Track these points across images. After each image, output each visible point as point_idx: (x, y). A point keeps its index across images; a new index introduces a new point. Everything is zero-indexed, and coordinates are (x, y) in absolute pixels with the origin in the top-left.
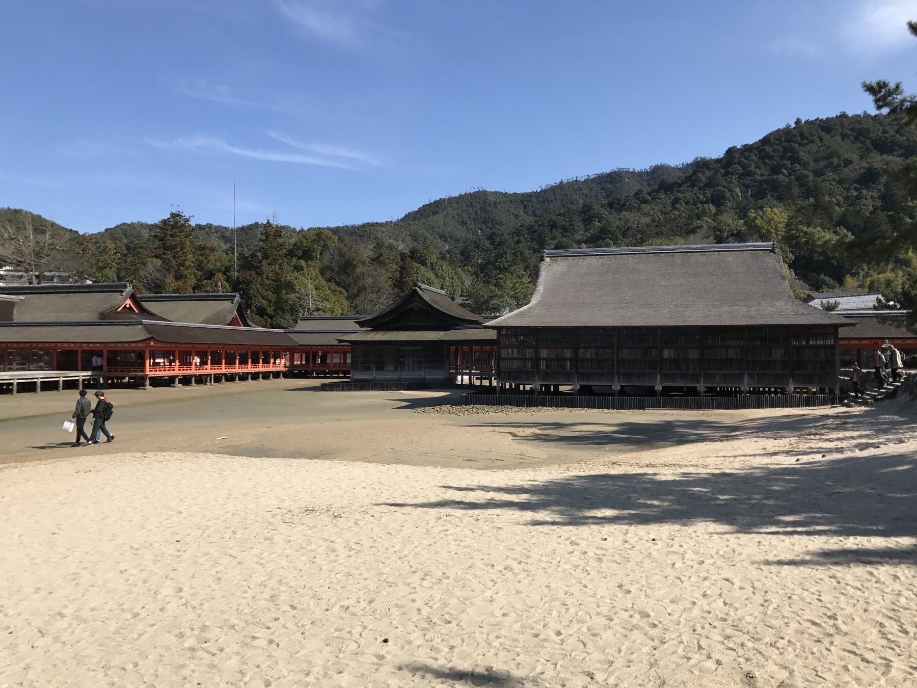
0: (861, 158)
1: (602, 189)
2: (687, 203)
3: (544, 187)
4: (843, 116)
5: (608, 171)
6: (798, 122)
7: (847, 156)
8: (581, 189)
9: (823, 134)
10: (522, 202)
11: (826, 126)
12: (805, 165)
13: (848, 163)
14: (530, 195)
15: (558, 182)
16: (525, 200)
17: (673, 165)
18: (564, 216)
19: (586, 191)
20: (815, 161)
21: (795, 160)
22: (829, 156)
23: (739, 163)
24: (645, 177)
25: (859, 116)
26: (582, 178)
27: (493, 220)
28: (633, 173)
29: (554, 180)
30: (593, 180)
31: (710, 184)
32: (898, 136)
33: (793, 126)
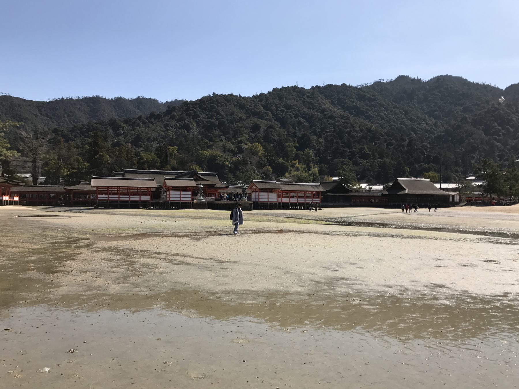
0: (248, 118)
1: (88, 106)
2: (172, 127)
3: (51, 100)
4: (232, 95)
6: (214, 94)
7: (239, 115)
8: (75, 104)
9: (226, 102)
10: (38, 107)
11: (229, 99)
12: (223, 116)
13: (241, 119)
14: (43, 103)
15: (61, 98)
16: (40, 105)
17: (127, 98)
18: (101, 124)
19: (79, 106)
20: (226, 115)
21: (218, 113)
22: (232, 114)
23: (192, 110)
26: (75, 97)
27: (20, 115)
28: (105, 99)
29: (58, 97)
31: (181, 119)
32: (256, 109)
33: (212, 95)
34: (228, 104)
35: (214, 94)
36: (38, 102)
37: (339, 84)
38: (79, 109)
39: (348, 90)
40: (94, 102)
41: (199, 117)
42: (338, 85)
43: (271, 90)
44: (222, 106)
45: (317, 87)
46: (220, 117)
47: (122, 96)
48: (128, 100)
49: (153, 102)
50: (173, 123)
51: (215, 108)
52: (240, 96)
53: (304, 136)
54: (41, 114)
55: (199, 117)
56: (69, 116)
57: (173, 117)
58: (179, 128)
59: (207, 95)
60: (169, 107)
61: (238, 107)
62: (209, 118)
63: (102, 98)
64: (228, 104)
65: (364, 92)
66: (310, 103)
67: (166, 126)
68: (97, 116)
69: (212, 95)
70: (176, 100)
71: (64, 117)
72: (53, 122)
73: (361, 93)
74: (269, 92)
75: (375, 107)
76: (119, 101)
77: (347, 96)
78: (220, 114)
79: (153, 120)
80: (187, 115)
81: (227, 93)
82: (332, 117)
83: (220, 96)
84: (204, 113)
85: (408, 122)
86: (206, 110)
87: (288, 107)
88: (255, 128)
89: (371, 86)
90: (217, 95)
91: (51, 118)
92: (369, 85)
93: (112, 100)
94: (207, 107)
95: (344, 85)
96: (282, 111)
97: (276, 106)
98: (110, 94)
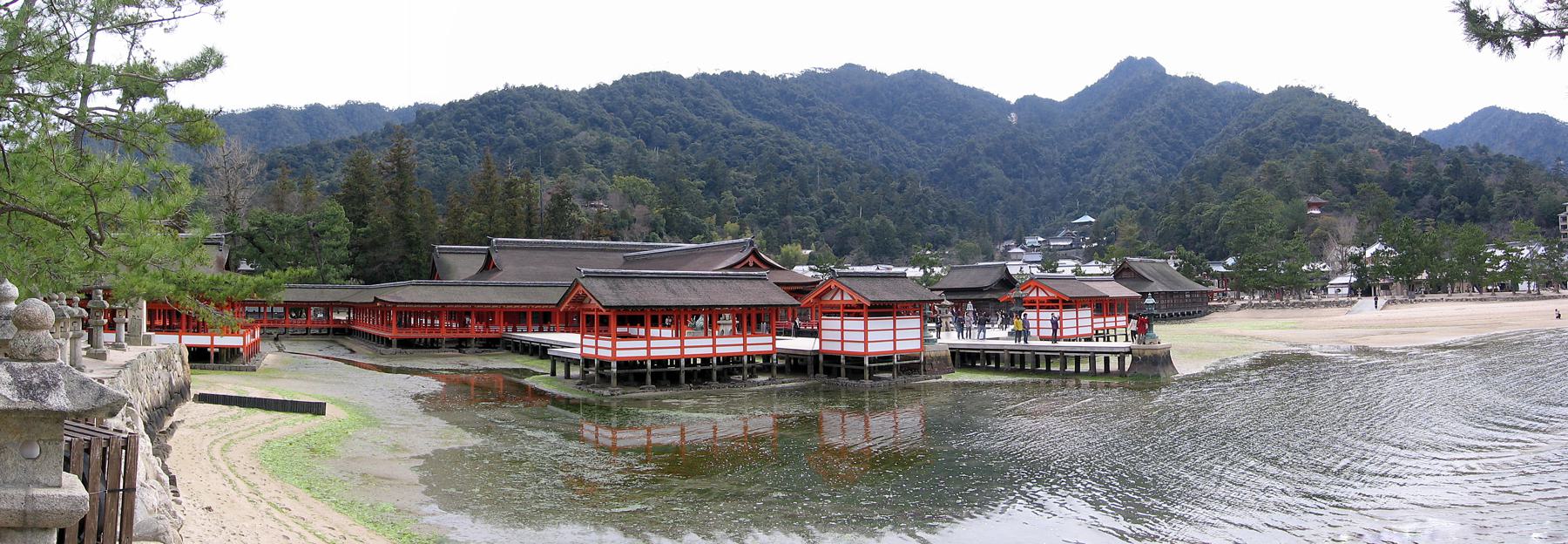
13: (568, 134)
37: (746, 72)
43: (618, 78)
45: (704, 75)
53: (712, 166)
60: (418, 113)
66: (696, 105)
73: (783, 89)
74: (616, 83)
75: (814, 115)
82: (748, 132)
85: (878, 149)
87: (657, 110)
88: (604, 149)
96: (647, 118)
97: (631, 107)
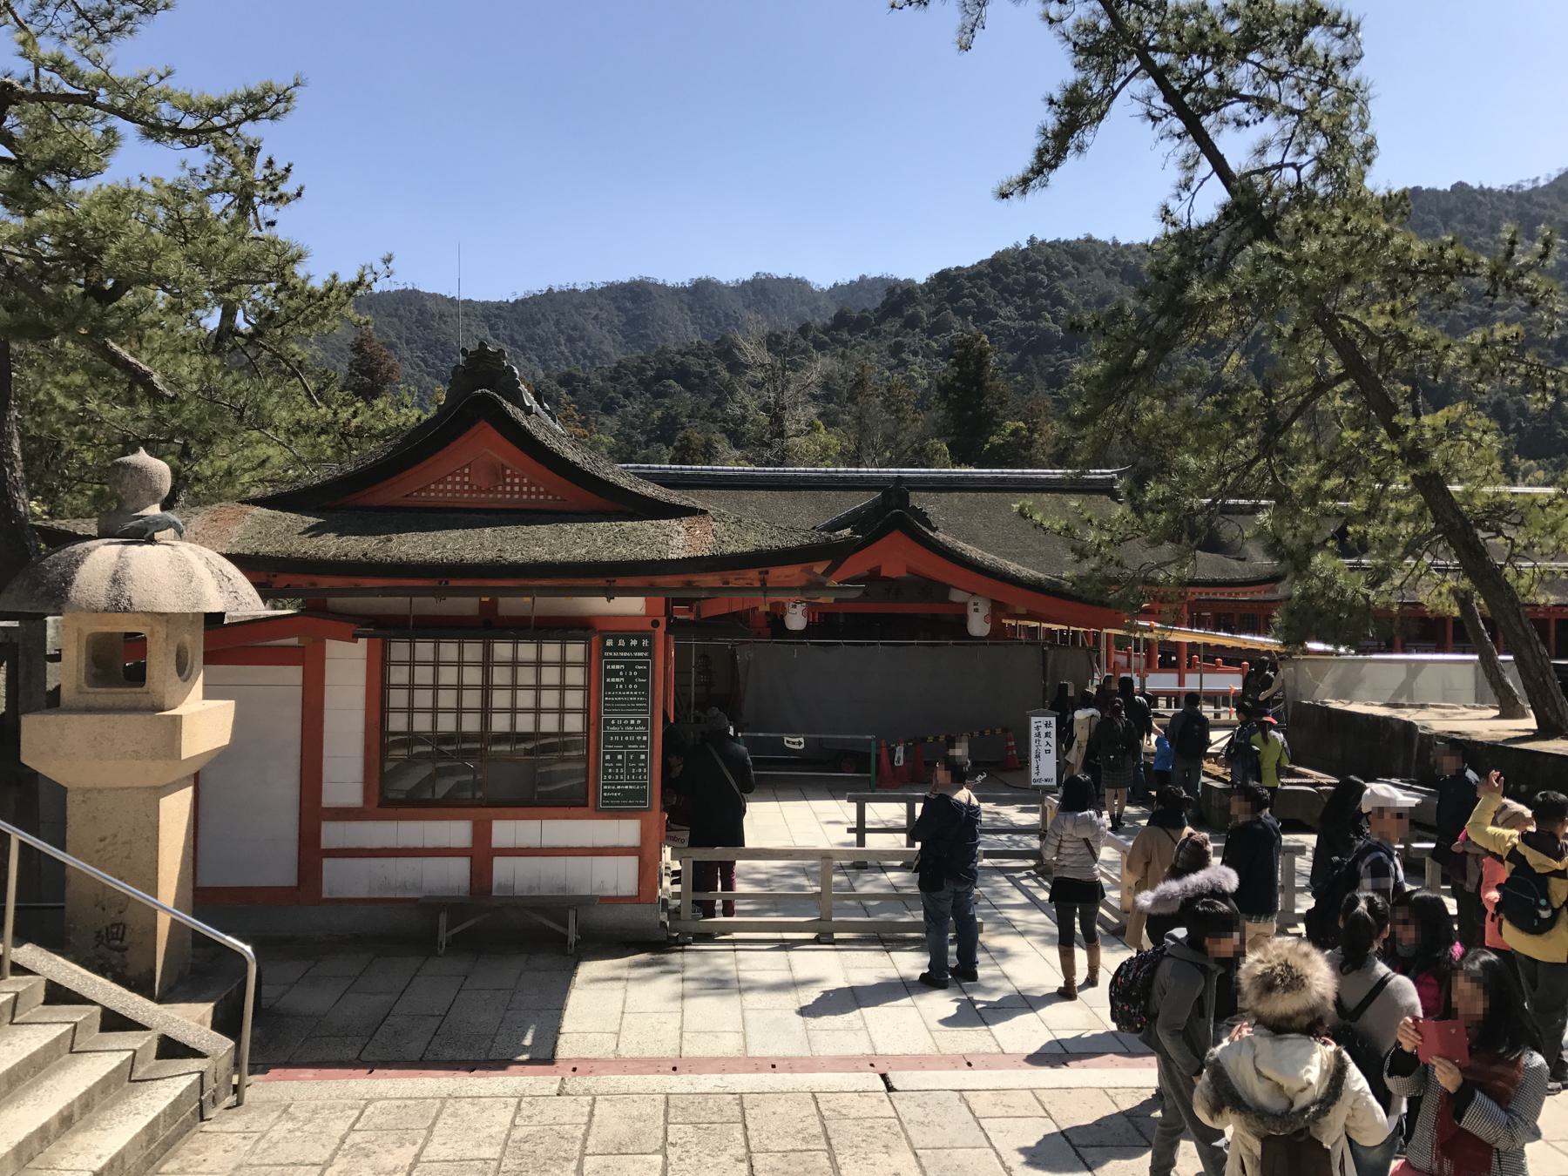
1: (618, 308)
2: (915, 354)
3: (520, 295)
4: (1089, 240)
5: (626, 280)
6: (1032, 240)
8: (584, 306)
10: (487, 318)
14: (499, 306)
15: (545, 289)
17: (724, 281)
18: (696, 356)
19: (594, 312)
21: (1058, 300)
24: (685, 297)
25: (1106, 244)
27: (444, 344)
28: (664, 286)
29: (538, 286)
30: (601, 292)
34: (1082, 268)
35: (1032, 240)
36: (485, 305)
37: (1444, 185)
38: (596, 318)
39: (1480, 204)
40: (633, 300)
41: (994, 315)
42: (1440, 188)
44: (1066, 276)
46: (1063, 312)
47: (711, 276)
48: (726, 287)
49: (797, 286)
50: (914, 339)
51: (1041, 284)
52: (1116, 244)
54: (496, 337)
55: (994, 315)
56: (570, 340)
57: (912, 322)
58: (938, 354)
59: (1010, 245)
61: (1118, 279)
62: (1025, 317)
63: (655, 284)
64: (1082, 268)
65: (1544, 206)
67: (896, 350)
68: (647, 337)
69: (1025, 246)
70: (863, 278)
71: (558, 344)
72: (529, 360)
76: (701, 293)
77: (1480, 226)
78: (1064, 303)
79: (846, 336)
80: (956, 312)
81: (1071, 233)
83: (1052, 245)
84: (1008, 304)
86: (1013, 293)
89: (1551, 185)
90: (1043, 242)
91: (523, 348)
92: (1542, 183)
93: (684, 289)
94: (1016, 282)
95: (1460, 188)
98: (675, 272)
